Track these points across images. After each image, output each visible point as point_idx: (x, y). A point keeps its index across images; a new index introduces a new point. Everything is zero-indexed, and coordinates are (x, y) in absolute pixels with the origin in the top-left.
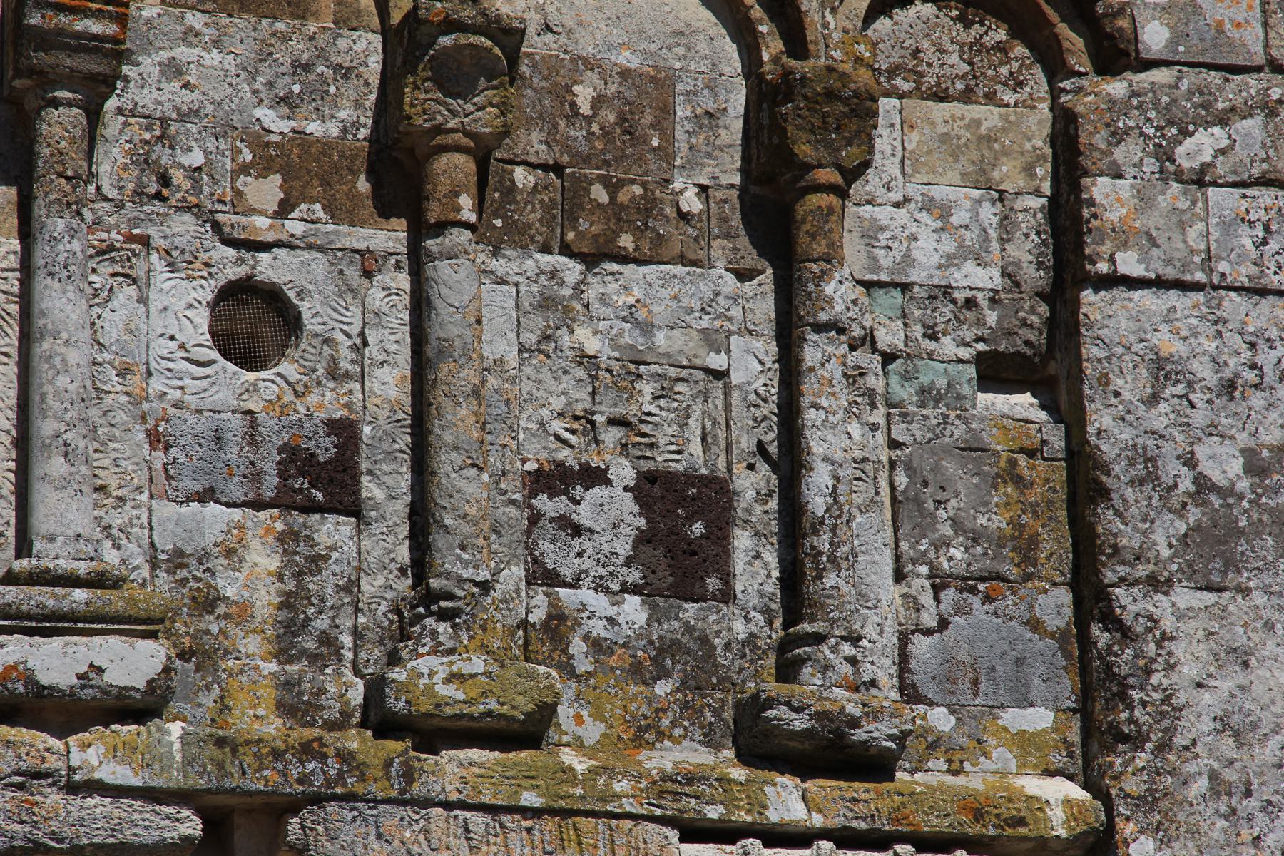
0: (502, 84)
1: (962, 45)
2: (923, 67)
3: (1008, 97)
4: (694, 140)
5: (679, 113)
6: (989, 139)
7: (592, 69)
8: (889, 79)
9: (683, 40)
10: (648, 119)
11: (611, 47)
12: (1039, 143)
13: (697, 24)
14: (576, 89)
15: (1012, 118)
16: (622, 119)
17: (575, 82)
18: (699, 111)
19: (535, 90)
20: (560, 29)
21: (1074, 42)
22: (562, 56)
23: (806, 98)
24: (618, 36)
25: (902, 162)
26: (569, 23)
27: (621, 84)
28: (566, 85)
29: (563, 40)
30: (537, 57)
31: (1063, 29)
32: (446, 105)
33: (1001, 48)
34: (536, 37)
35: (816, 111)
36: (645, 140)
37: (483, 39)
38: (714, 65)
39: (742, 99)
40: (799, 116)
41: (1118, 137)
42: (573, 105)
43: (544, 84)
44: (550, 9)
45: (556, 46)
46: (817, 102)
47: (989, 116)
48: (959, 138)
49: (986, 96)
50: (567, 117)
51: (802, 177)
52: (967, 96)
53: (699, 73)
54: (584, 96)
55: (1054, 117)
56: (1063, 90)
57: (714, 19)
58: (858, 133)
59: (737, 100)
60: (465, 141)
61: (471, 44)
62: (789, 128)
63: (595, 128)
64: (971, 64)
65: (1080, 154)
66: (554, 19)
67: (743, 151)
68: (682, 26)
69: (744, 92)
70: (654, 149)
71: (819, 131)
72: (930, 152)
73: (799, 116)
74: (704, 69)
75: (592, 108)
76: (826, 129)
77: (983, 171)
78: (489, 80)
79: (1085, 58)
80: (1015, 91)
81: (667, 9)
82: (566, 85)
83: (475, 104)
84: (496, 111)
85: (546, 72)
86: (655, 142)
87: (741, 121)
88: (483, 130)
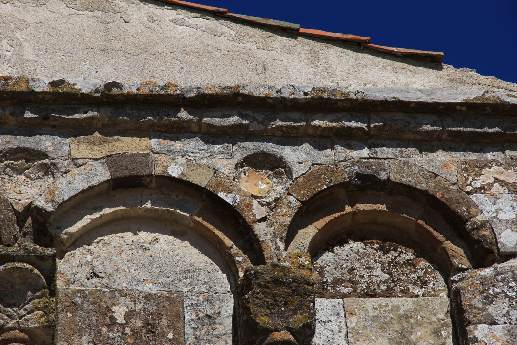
0: (44, 294)
1: (383, 264)
2: (357, 278)
3: (418, 291)
4: (198, 333)
5: (187, 317)
6: (406, 317)
7: (126, 296)
8: (334, 288)
9: (189, 275)
10: (165, 322)
11: (138, 282)
12: (442, 316)
13: (198, 265)
14: (114, 308)
15: (422, 303)
16: (147, 323)
17: (113, 305)
18: (201, 315)
19: (85, 311)
20: (103, 275)
21: (457, 254)
22: (104, 290)
23: (260, 285)
24: (143, 275)
25: (347, 336)
26: (109, 269)
27: (145, 303)
28: (107, 307)
29: (105, 281)
30: (87, 292)
31: (448, 244)
32: (5, 312)
33: (408, 263)
34: (86, 281)
35: (269, 294)
36: (163, 335)
37: (25, 265)
38: (211, 287)
39: (232, 306)
40: (257, 298)
41: (490, 300)
42: (112, 318)
43: (91, 307)
44: (95, 263)
45: (100, 285)
46: (268, 288)
47: (406, 304)
48: (385, 318)
49: (402, 291)
50: (108, 326)
51: (265, 339)
52: (389, 293)
53: (201, 293)
54: (119, 312)
55: (451, 301)
56: (454, 281)
57: (210, 261)
58: (300, 306)
59: (228, 306)
60: (18, 333)
61: (17, 268)
62: (251, 307)
63: (128, 330)
64: (390, 274)
65: (464, 311)
66: (99, 269)
67: (234, 337)
68: (188, 267)
69: (232, 301)
70: (170, 340)
71: (273, 307)
72: (365, 327)
73: (257, 298)
74: (204, 290)
75: (125, 319)
76: (277, 305)
77: (405, 336)
78: (34, 293)
79: (465, 260)
80: (422, 287)
81: (178, 257)
82: (107, 307)
83: (26, 310)
84: (41, 313)
85: (93, 300)
86: (170, 336)
87: (231, 319)
88: (33, 326)
